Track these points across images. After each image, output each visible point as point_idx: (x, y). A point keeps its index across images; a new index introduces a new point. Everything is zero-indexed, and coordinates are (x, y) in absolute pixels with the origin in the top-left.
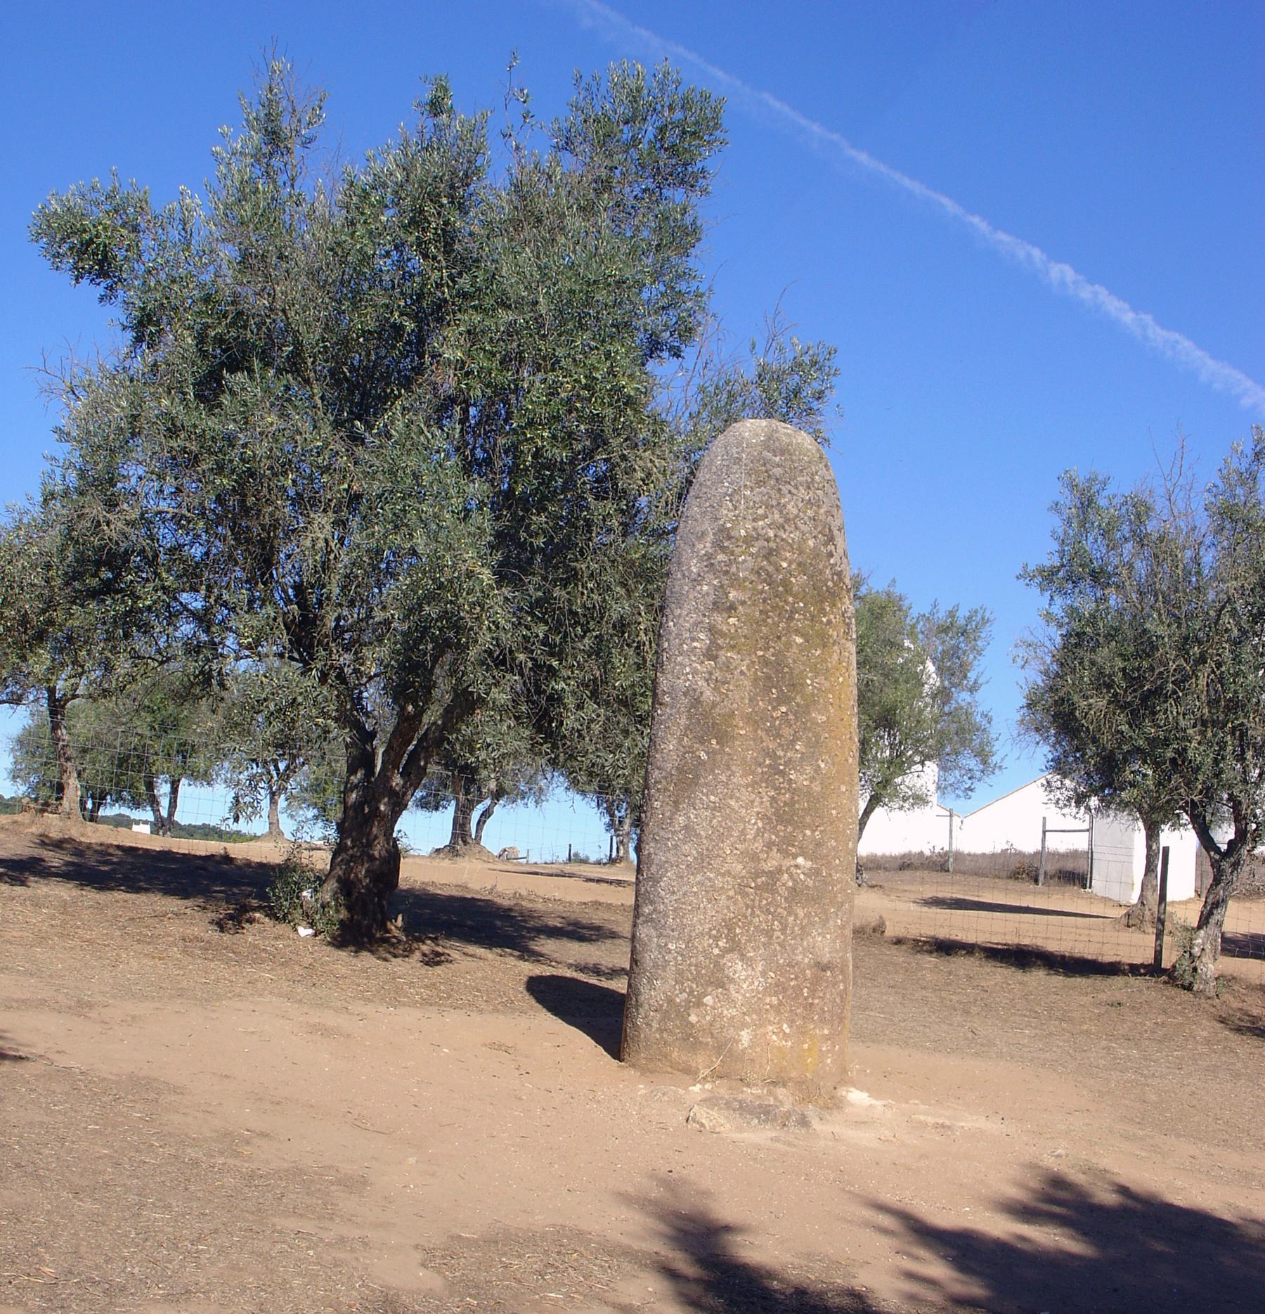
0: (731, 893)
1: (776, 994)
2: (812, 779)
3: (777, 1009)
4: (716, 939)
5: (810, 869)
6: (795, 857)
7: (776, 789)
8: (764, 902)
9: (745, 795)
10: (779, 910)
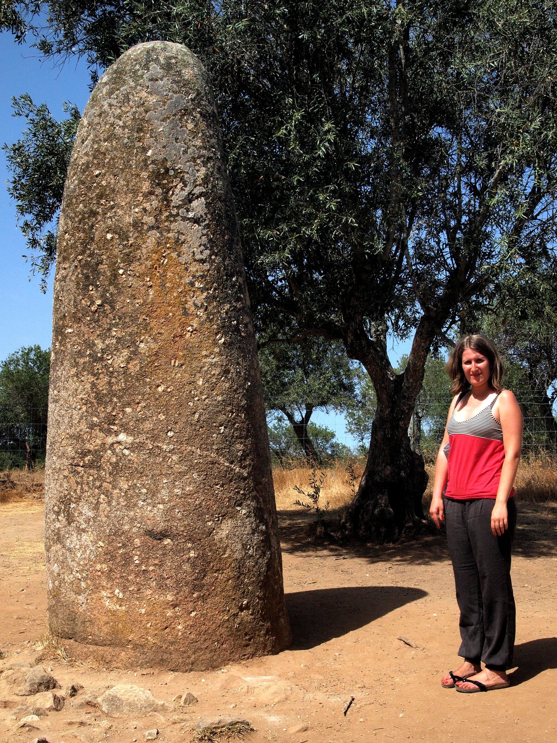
0: (66, 473)
1: (105, 562)
2: (129, 360)
3: (109, 575)
4: (58, 513)
5: (132, 444)
6: (117, 434)
7: (94, 375)
8: (91, 478)
9: (73, 385)
10: (105, 484)
